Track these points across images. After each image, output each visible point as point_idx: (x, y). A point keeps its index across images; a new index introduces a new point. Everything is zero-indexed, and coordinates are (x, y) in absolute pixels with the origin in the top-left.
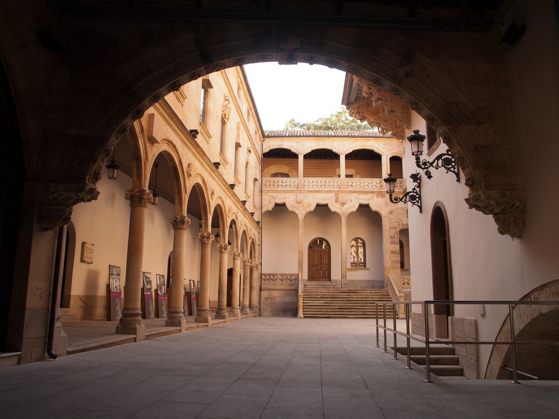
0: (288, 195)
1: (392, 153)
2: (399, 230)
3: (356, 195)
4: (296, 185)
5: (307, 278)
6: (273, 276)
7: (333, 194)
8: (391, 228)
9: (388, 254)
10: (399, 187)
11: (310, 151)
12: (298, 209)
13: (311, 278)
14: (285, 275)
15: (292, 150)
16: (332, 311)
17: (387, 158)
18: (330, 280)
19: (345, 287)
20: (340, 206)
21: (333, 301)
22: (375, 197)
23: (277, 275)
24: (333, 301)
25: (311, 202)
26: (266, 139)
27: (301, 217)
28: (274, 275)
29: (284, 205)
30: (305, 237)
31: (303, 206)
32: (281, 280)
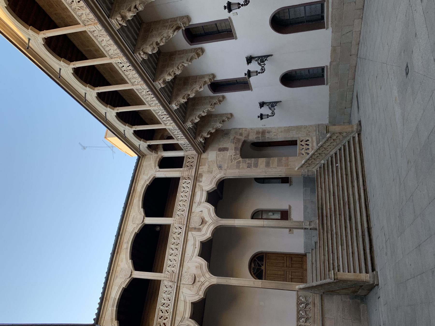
0: (181, 297)
3: (194, 206)
4: (170, 284)
7: (190, 233)
8: (238, 167)
9: (270, 170)
10: (193, 160)
11: (130, 262)
13: (302, 280)
14: (298, 312)
15: (124, 286)
17: (159, 171)
18: (305, 255)
20: (206, 226)
22: (201, 184)
25: (195, 264)
27: (215, 280)
29: (194, 304)
30: (244, 280)
31: (200, 277)
32: (307, 319)
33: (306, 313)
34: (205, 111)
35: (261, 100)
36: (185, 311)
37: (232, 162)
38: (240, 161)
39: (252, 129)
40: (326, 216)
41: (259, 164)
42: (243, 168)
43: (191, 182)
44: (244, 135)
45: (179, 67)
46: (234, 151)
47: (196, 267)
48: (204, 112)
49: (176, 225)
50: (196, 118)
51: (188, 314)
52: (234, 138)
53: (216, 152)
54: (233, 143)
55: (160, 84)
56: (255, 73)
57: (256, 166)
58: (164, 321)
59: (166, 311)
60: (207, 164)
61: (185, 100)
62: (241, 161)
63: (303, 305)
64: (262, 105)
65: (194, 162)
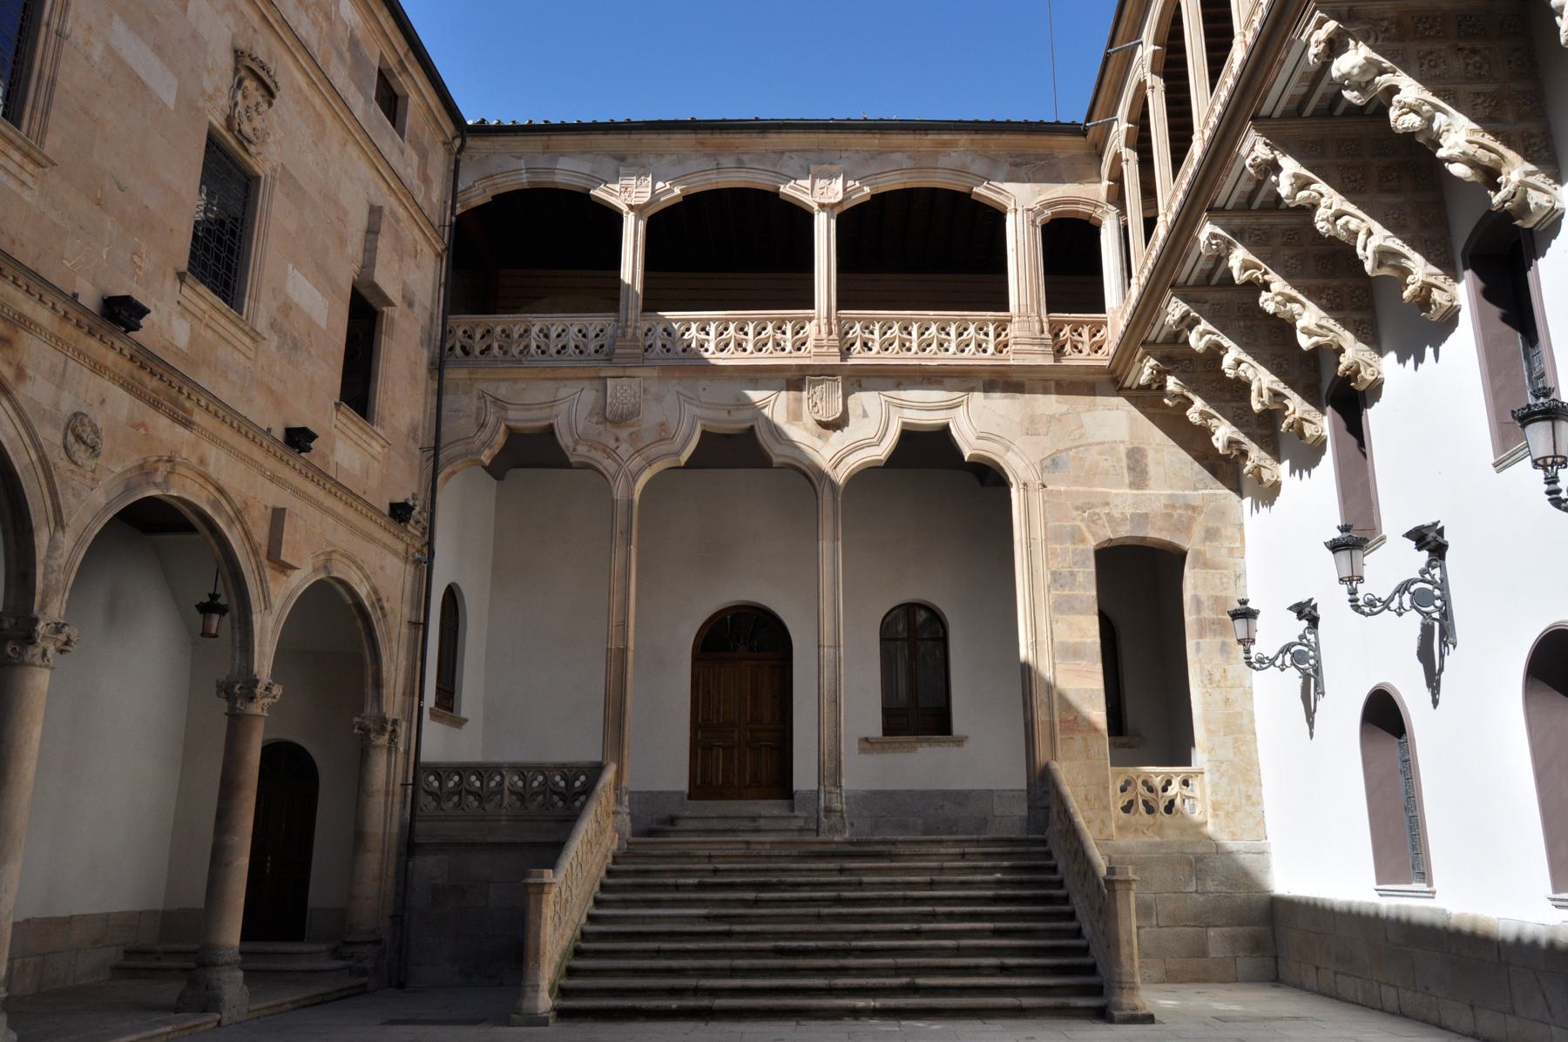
1: (1050, 205)
2: (1092, 544)
5: (683, 786)
6: (480, 777)
8: (1054, 535)
10: (1086, 349)
12: (610, 453)
14: (540, 769)
16: (733, 972)
19: (833, 829)
21: (756, 903)
23: (497, 769)
24: (756, 903)
26: (470, 142)
28: (482, 771)
31: (634, 438)
33: (538, 794)
34: (1243, 366)
35: (1320, 612)
36: (528, 407)
37: (1077, 508)
38: (1083, 540)
39: (1238, 577)
40: (842, 871)
41: (1069, 618)
42: (1050, 555)
43: (988, 358)
44: (1207, 548)
45: (1340, 222)
46: (1129, 512)
47: (662, 424)
48: (1239, 363)
49: (810, 329)
50: (1202, 335)
51: (522, 418)
52: (1194, 509)
53: (1126, 438)
54: (1166, 506)
55: (1252, 149)
56: (1346, 573)
57: (1063, 606)
58: (496, 345)
59: (564, 347)
60: (1064, 408)
61: (1239, 276)
62: (1081, 547)
63: (562, 784)
64: (1307, 612)
65: (1076, 355)
